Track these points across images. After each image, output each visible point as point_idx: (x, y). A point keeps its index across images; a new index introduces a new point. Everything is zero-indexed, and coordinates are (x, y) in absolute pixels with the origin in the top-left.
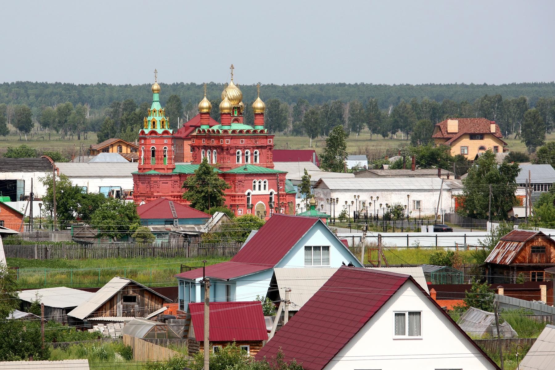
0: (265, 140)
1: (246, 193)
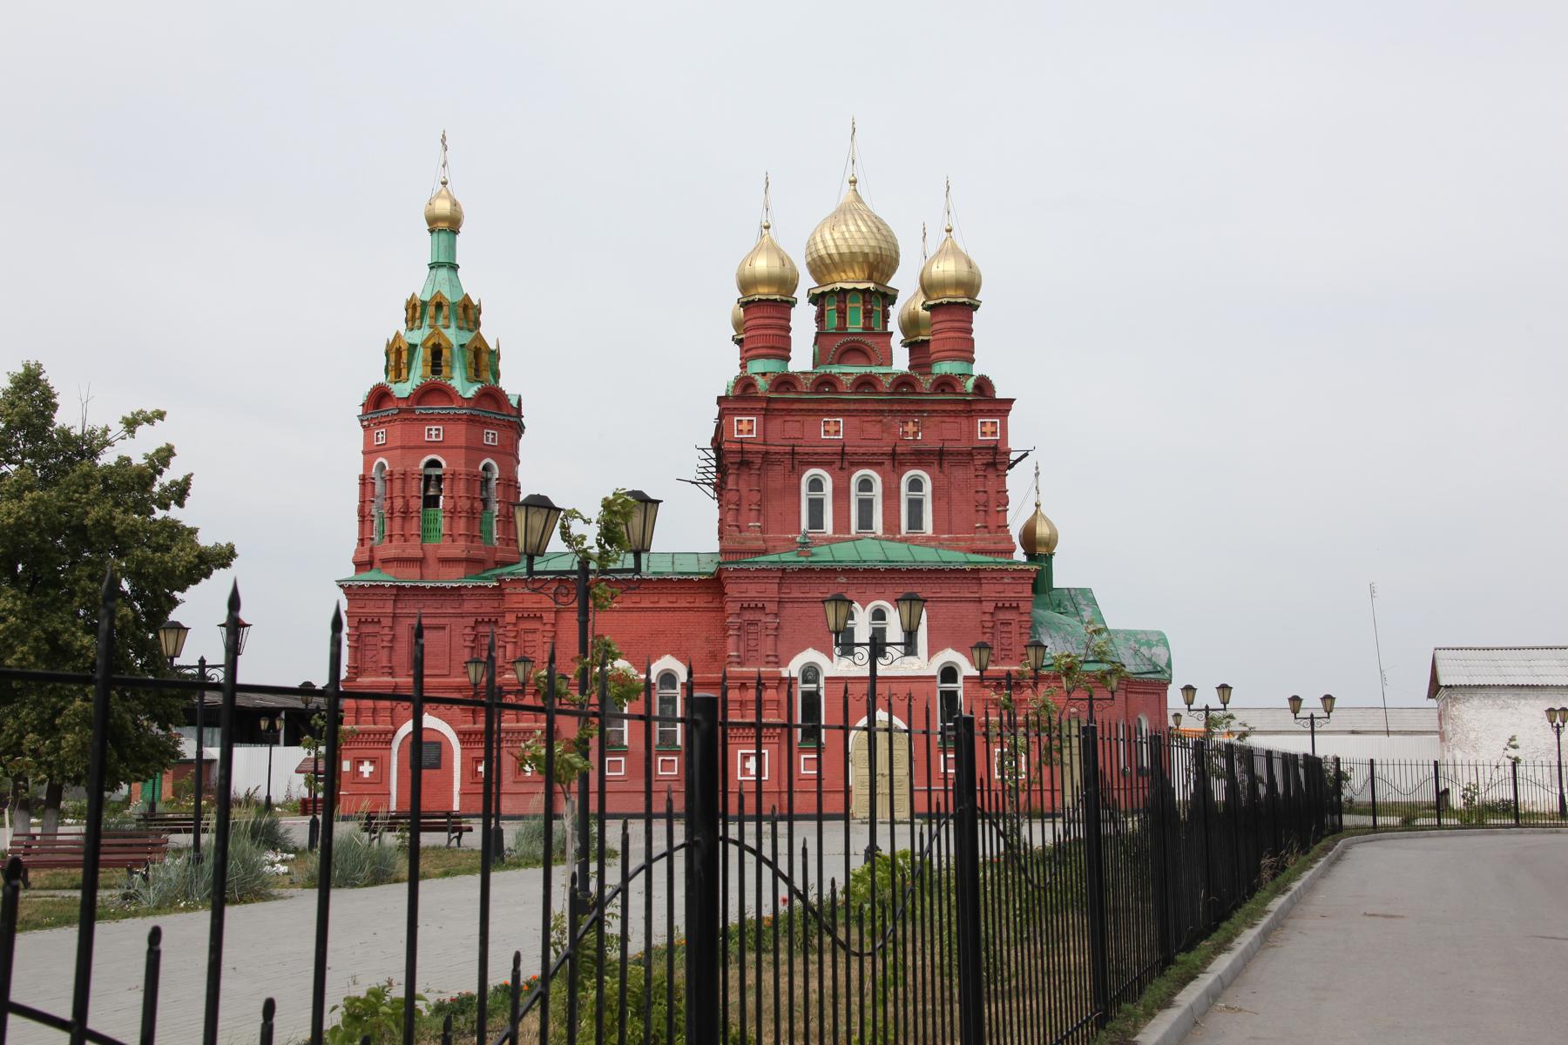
0: (964, 422)
1: (793, 668)
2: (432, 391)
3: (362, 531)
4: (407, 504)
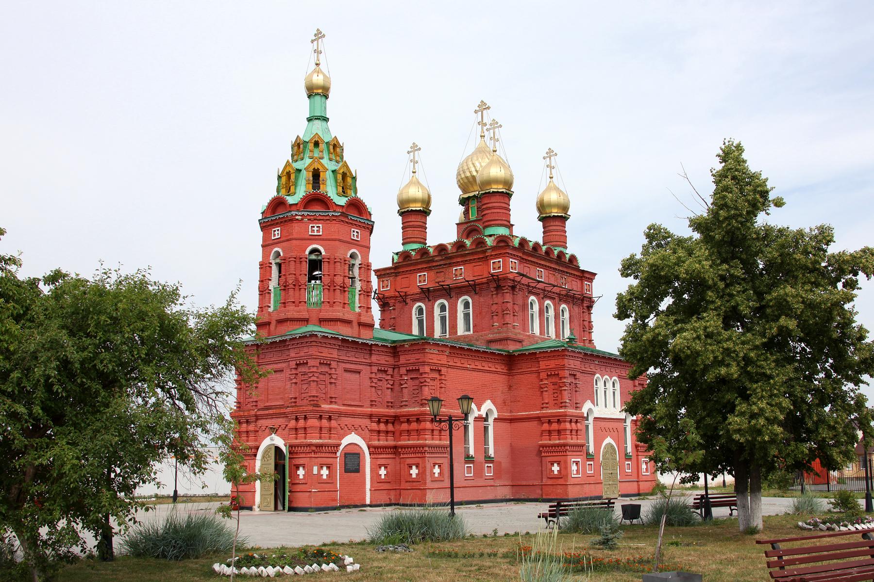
2: (316, 200)
3: (261, 301)
4: (297, 280)
